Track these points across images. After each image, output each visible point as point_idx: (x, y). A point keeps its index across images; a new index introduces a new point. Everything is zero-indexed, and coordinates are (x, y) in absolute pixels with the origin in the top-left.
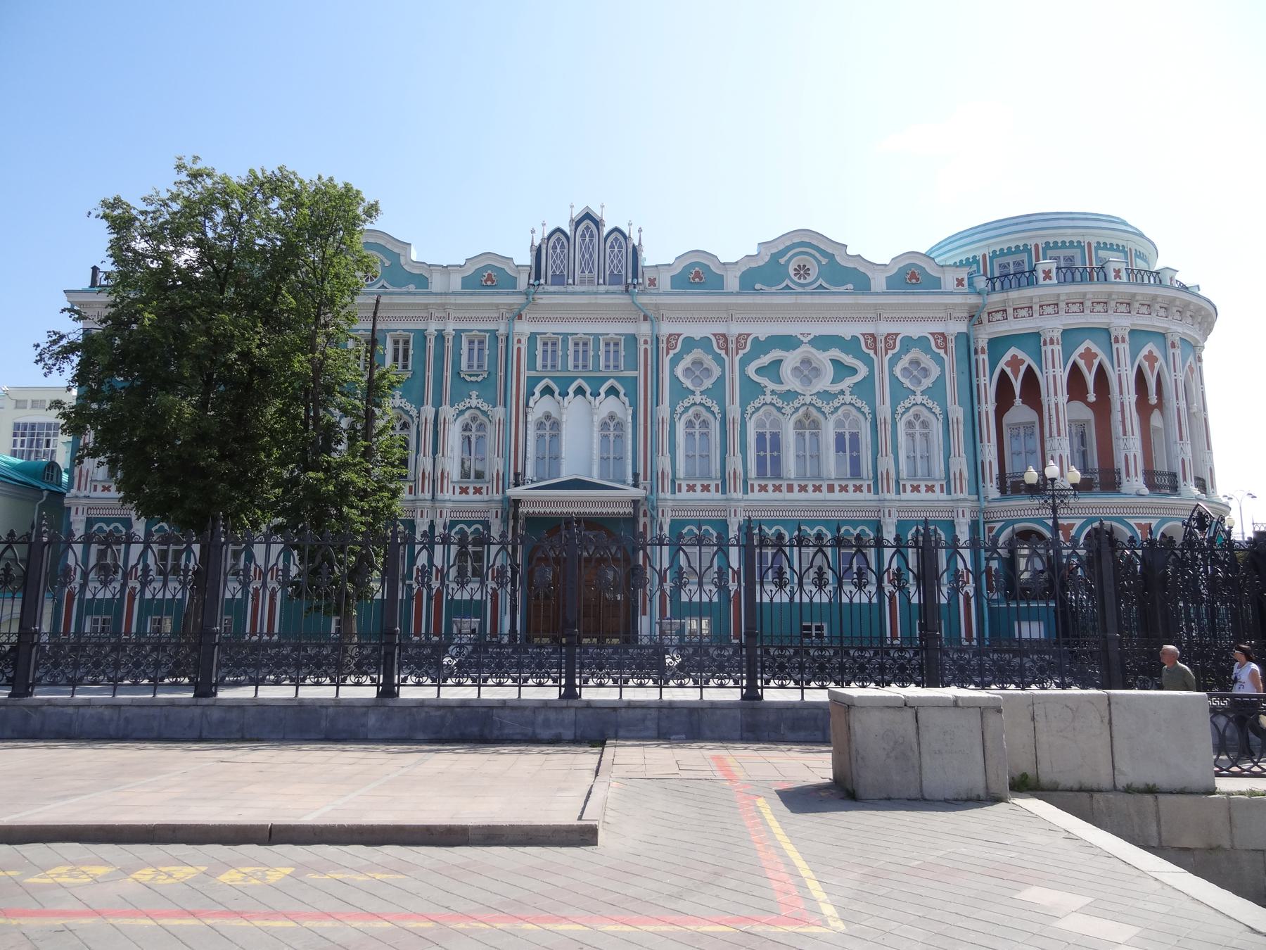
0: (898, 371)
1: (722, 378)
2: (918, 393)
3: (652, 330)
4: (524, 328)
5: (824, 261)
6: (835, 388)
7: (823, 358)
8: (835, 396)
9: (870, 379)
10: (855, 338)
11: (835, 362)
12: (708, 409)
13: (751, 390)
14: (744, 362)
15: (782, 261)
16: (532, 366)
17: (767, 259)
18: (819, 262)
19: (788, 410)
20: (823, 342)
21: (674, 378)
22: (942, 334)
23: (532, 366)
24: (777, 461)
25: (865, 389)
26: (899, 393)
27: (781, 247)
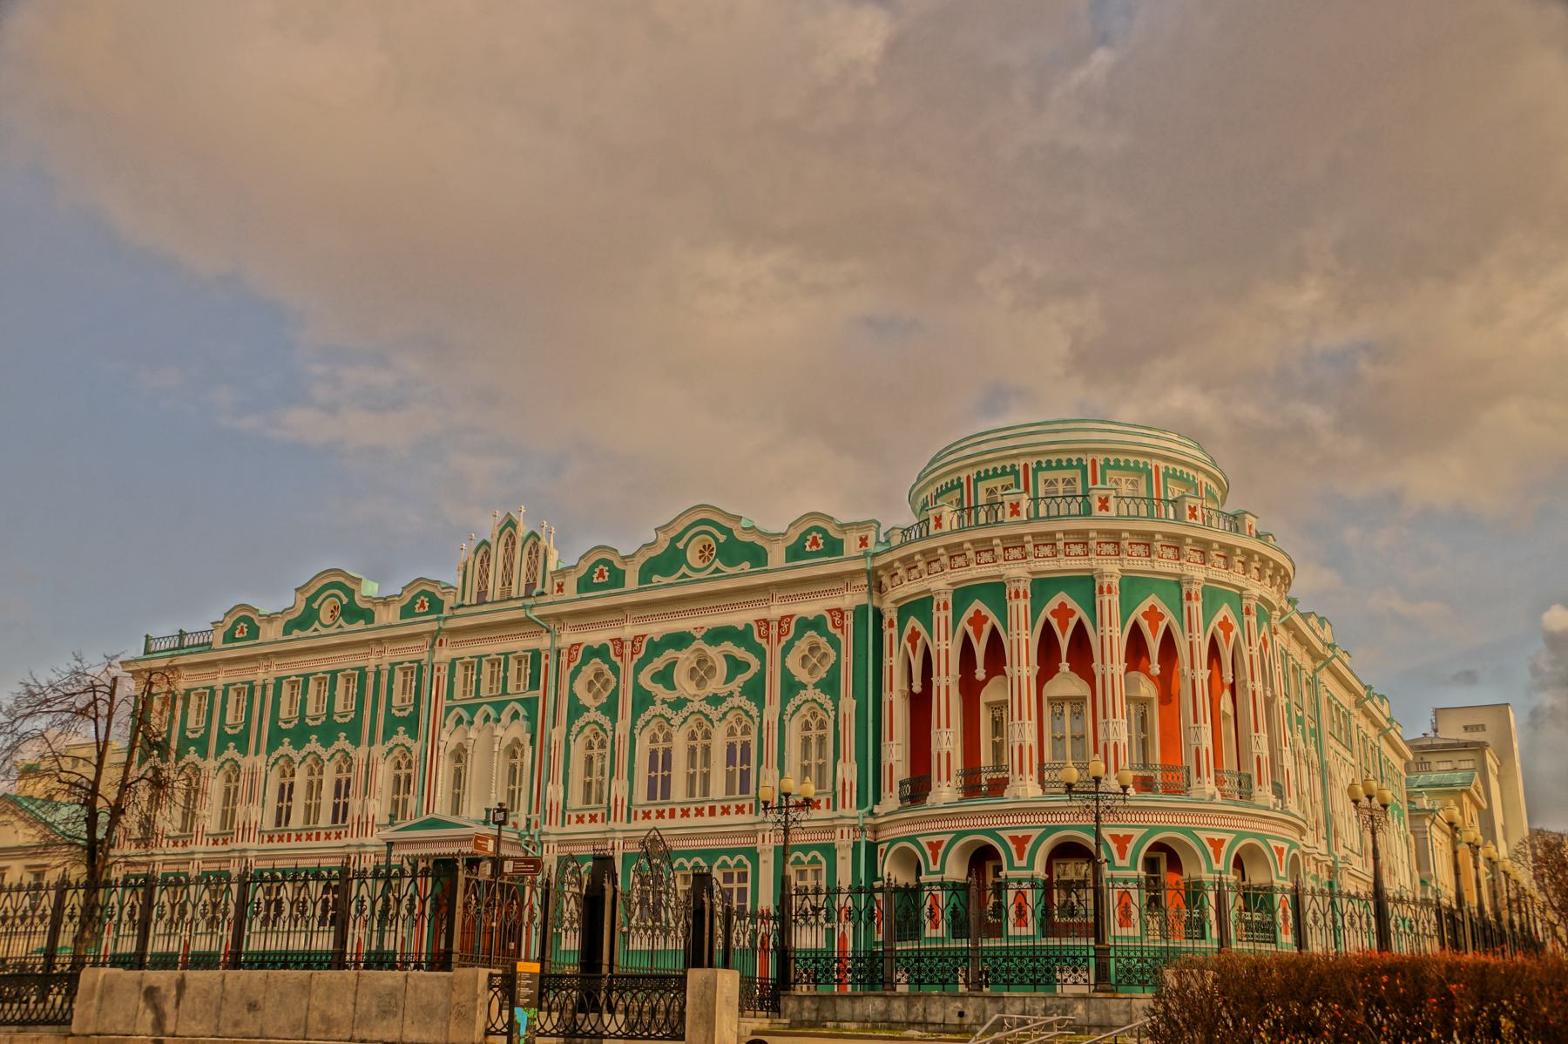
0: (793, 662)
1: (616, 691)
2: (810, 687)
3: (553, 642)
4: (444, 654)
5: (722, 538)
6: (723, 690)
7: (715, 653)
8: (724, 699)
9: (760, 677)
10: (748, 626)
11: (729, 658)
12: (601, 726)
13: (643, 700)
14: (638, 669)
15: (680, 545)
16: (450, 695)
17: (666, 545)
18: (716, 540)
19: (677, 720)
20: (717, 636)
21: (573, 697)
22: (839, 610)
23: (450, 695)
24: (667, 781)
25: (755, 690)
26: (791, 687)
27: (680, 529)
